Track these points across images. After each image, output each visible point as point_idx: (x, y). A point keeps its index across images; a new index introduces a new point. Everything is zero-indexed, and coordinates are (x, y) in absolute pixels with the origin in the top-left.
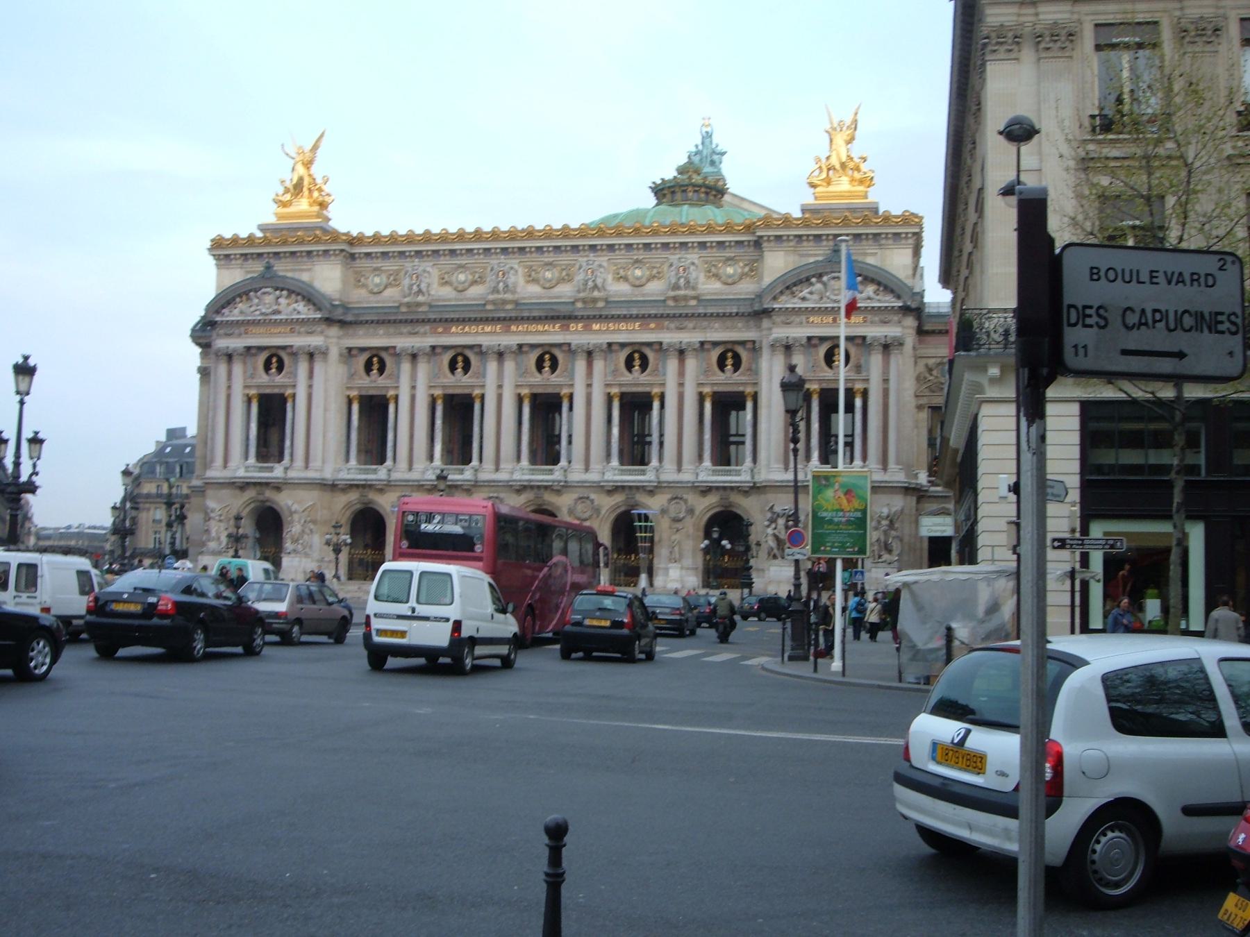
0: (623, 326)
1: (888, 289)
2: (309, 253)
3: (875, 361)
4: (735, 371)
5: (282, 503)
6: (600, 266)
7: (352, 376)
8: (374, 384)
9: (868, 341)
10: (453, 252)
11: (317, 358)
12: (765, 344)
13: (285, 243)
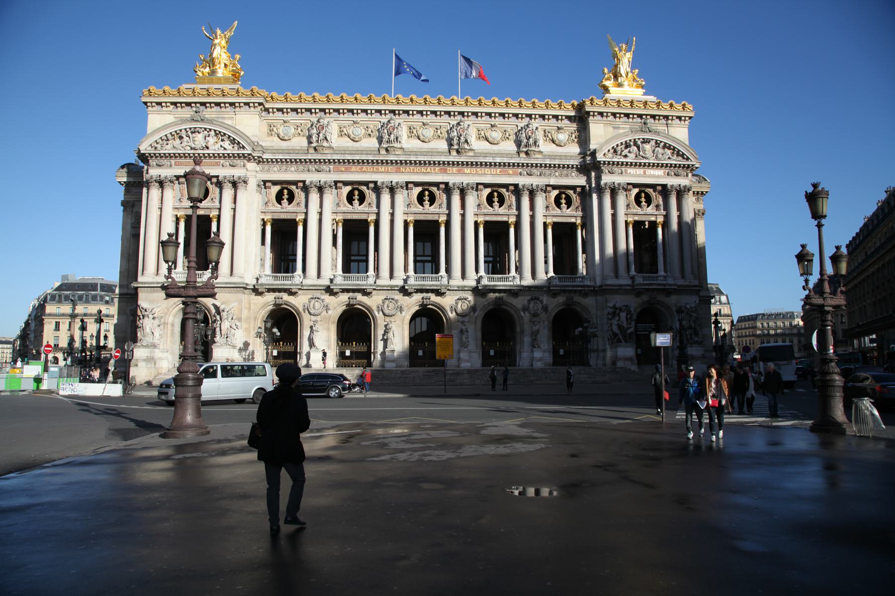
0: (487, 170)
1: (680, 154)
2: (232, 104)
8: (286, 210)
9: (669, 187)
10: (351, 111)
11: (241, 187)
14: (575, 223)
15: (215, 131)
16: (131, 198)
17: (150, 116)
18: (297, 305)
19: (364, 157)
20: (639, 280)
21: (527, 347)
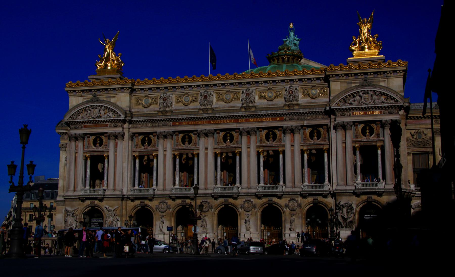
2: (114, 89)
4: (318, 139)
6: (252, 92)
10: (182, 87)
13: (102, 84)
14: (323, 149)
15: (105, 106)
17: (70, 98)
18: (152, 206)
19: (189, 116)
21: (287, 231)
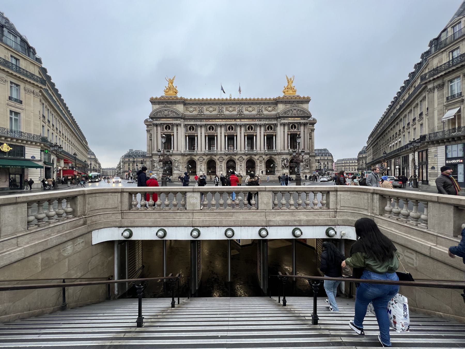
3: (302, 128)
5: (172, 159)
7: (187, 131)
8: (191, 132)
12: (279, 124)
16: (149, 129)
20: (291, 151)
21: (258, 170)
